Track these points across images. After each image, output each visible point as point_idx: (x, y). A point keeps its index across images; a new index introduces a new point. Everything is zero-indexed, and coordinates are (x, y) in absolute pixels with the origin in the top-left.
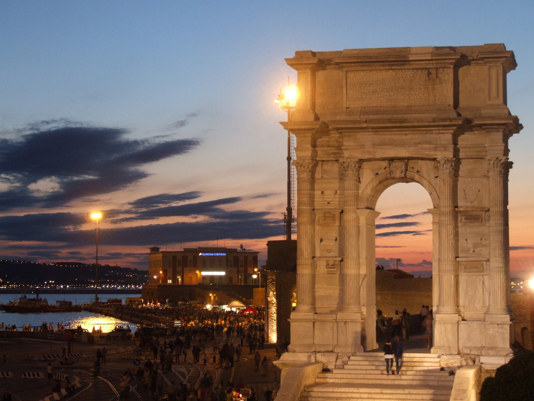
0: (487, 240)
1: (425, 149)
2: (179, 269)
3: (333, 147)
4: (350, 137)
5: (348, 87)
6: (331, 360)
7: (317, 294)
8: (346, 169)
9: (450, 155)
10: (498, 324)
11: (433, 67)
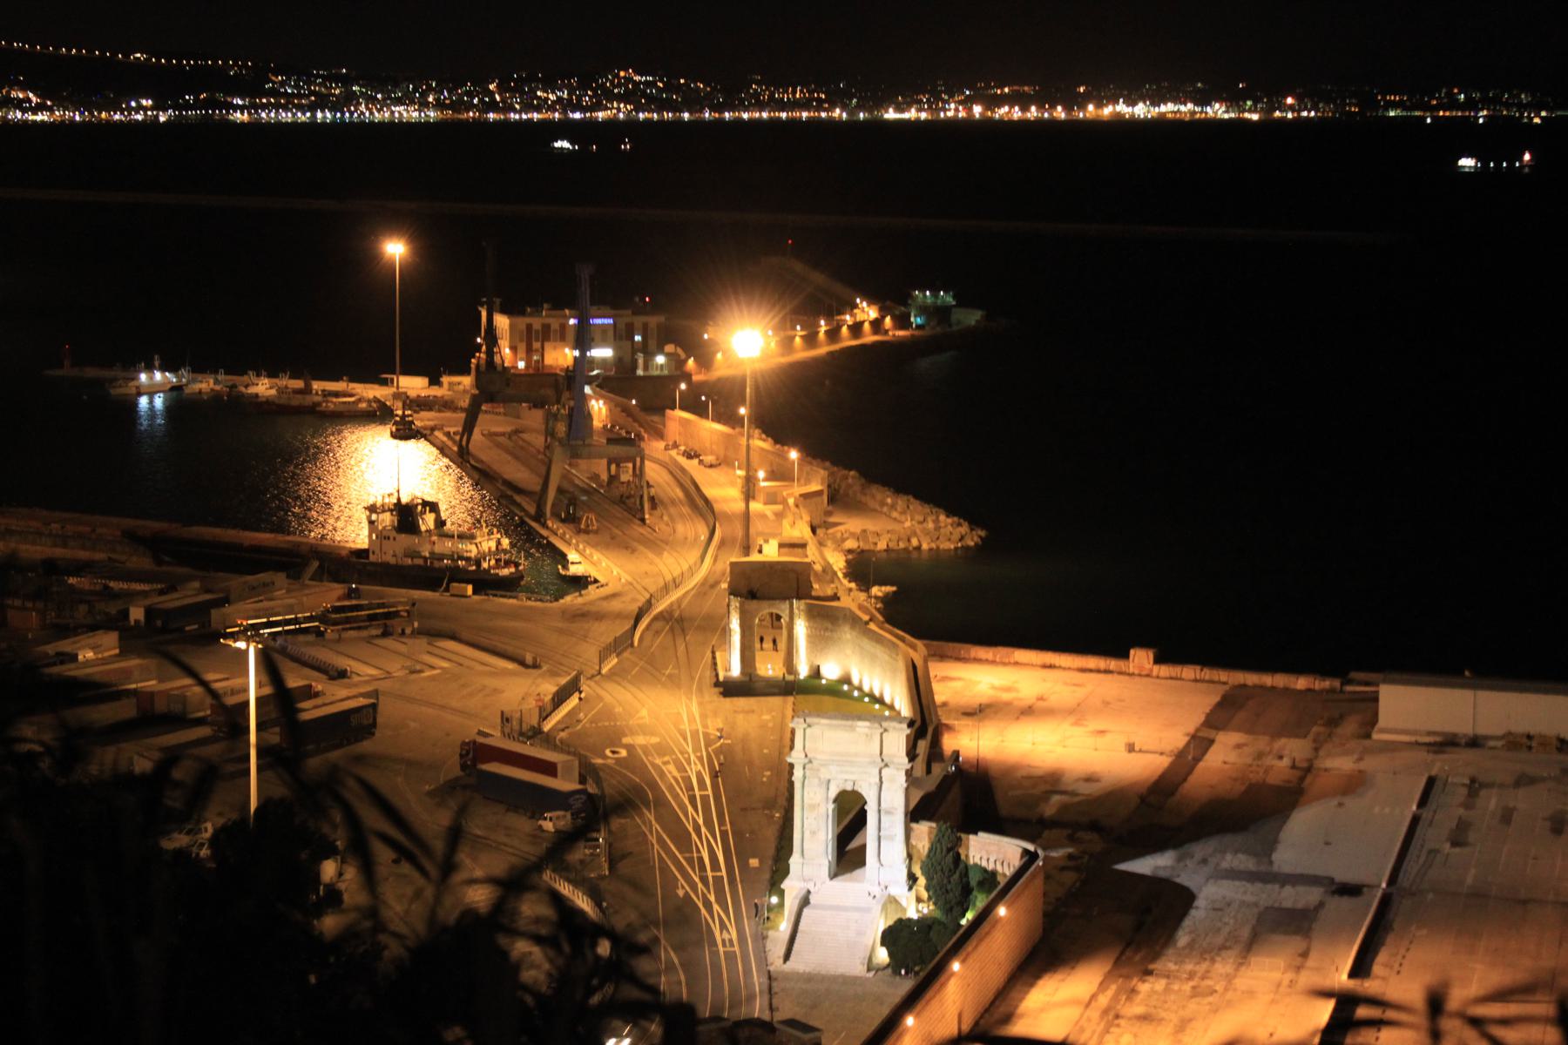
2: (537, 345)
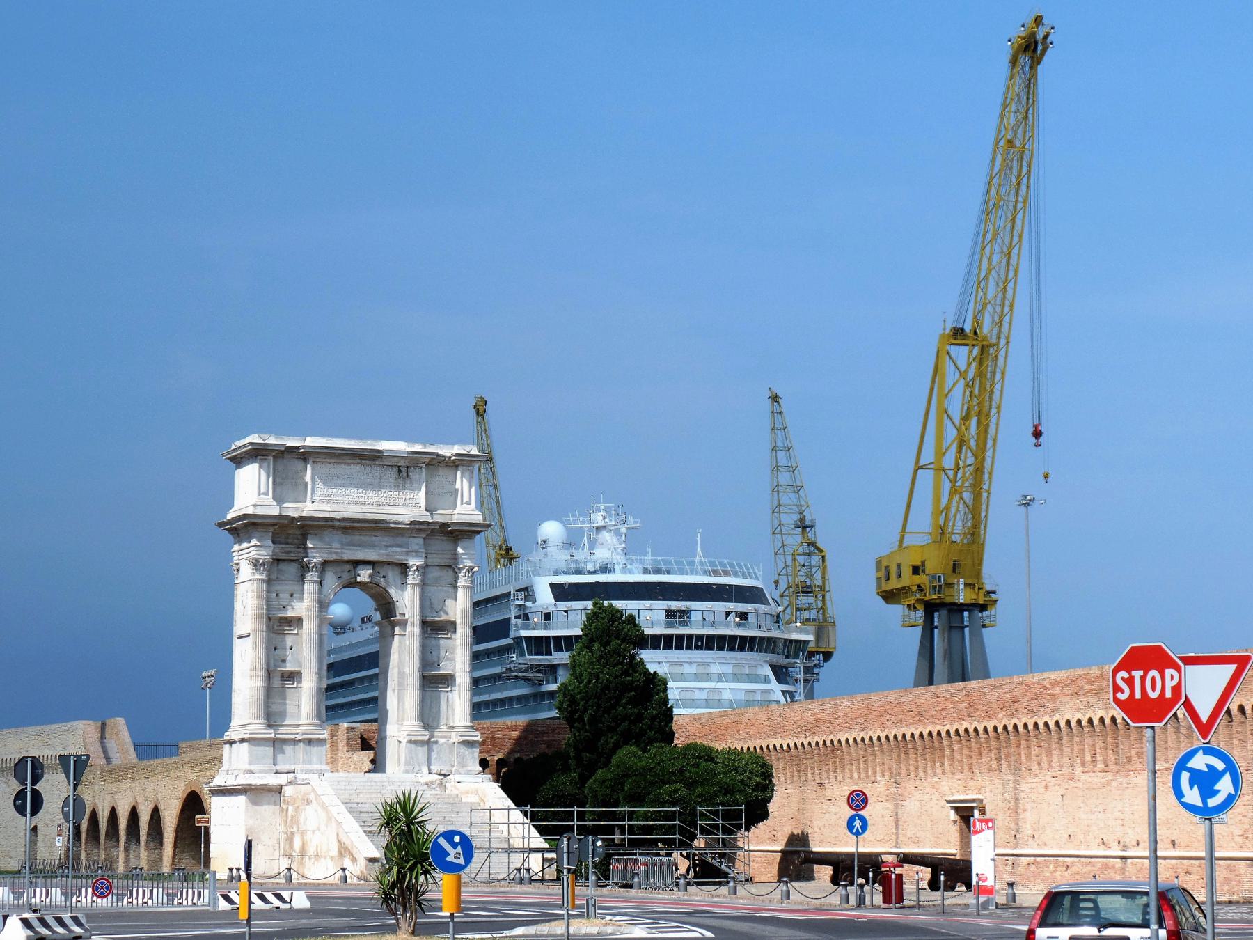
1: (396, 552)
3: (292, 544)
4: (316, 535)
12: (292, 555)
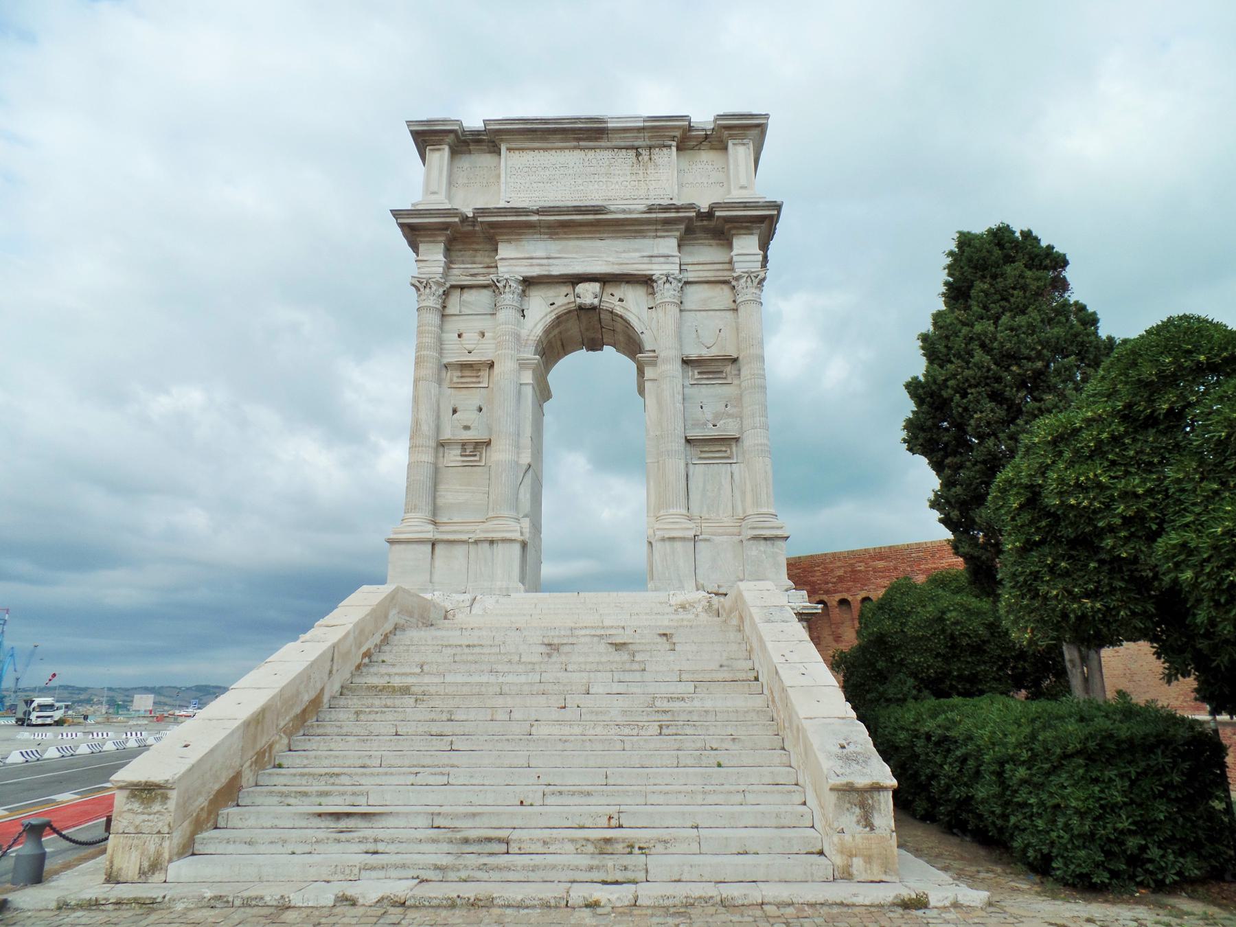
0: (735, 407)
5: (509, 170)
6: (462, 605)
7: (440, 502)
8: (502, 290)
9: (674, 269)
10: (765, 539)
11: (644, 143)
12: (481, 278)
